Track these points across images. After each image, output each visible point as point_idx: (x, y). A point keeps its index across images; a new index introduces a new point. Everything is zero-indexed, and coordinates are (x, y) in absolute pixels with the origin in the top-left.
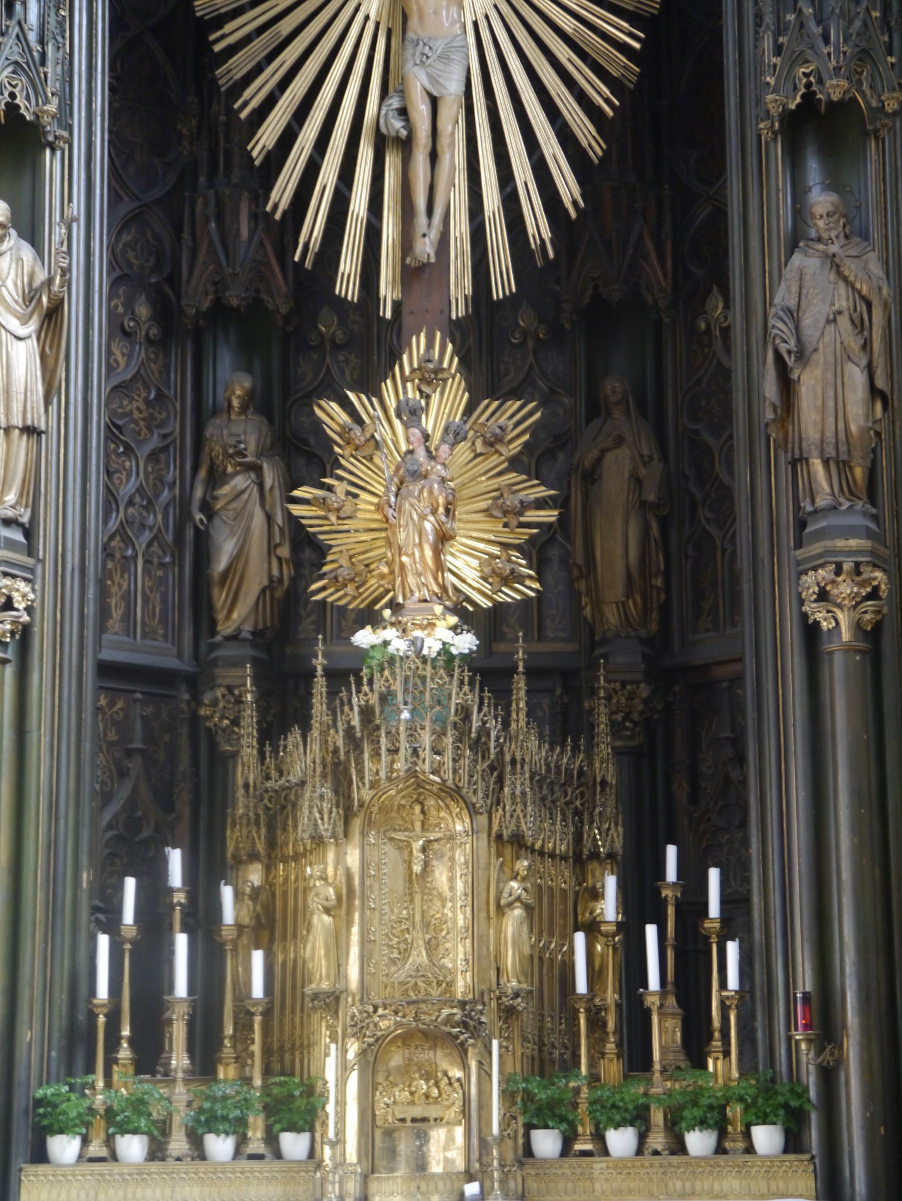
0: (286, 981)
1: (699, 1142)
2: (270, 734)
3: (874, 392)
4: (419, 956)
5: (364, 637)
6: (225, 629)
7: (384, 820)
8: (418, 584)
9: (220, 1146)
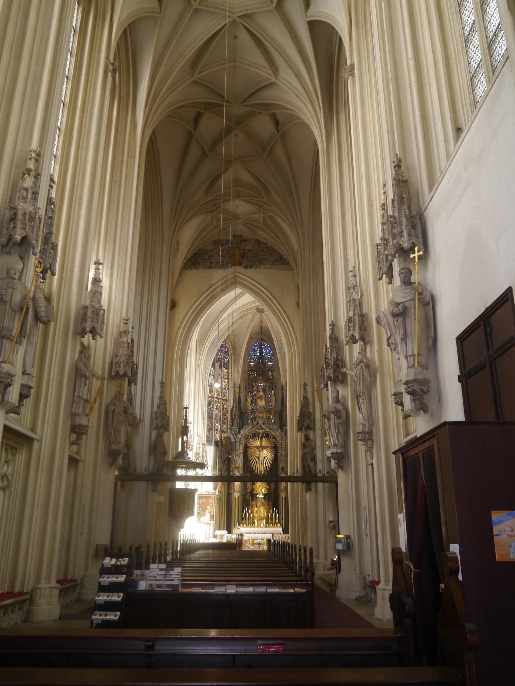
0: (253, 516)
7: (258, 507)
8: (260, 492)
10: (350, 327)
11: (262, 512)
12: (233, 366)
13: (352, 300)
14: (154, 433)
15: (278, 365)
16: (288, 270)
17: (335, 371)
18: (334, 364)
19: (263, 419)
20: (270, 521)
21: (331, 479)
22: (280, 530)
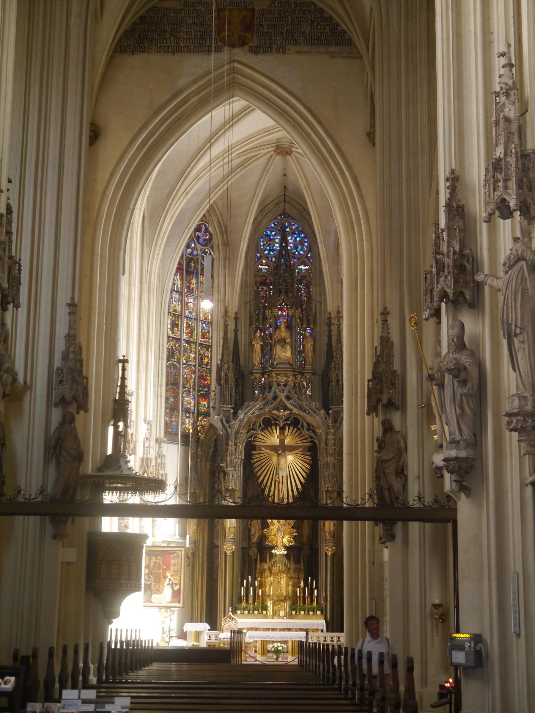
0: (264, 593)
1: (311, 613)
2: (261, 562)
3: (334, 525)
4: (279, 591)
5: (273, 551)
6: (253, 542)
7: (275, 575)
8: (279, 543)
9: (256, 612)
10: (496, 181)
11: (284, 586)
12: (222, 274)
13: (502, 123)
14: (56, 415)
15: (321, 272)
16: (349, 57)
17: (456, 282)
18: (455, 266)
19: (288, 388)
20: (299, 603)
21: (441, 515)
22: (321, 623)
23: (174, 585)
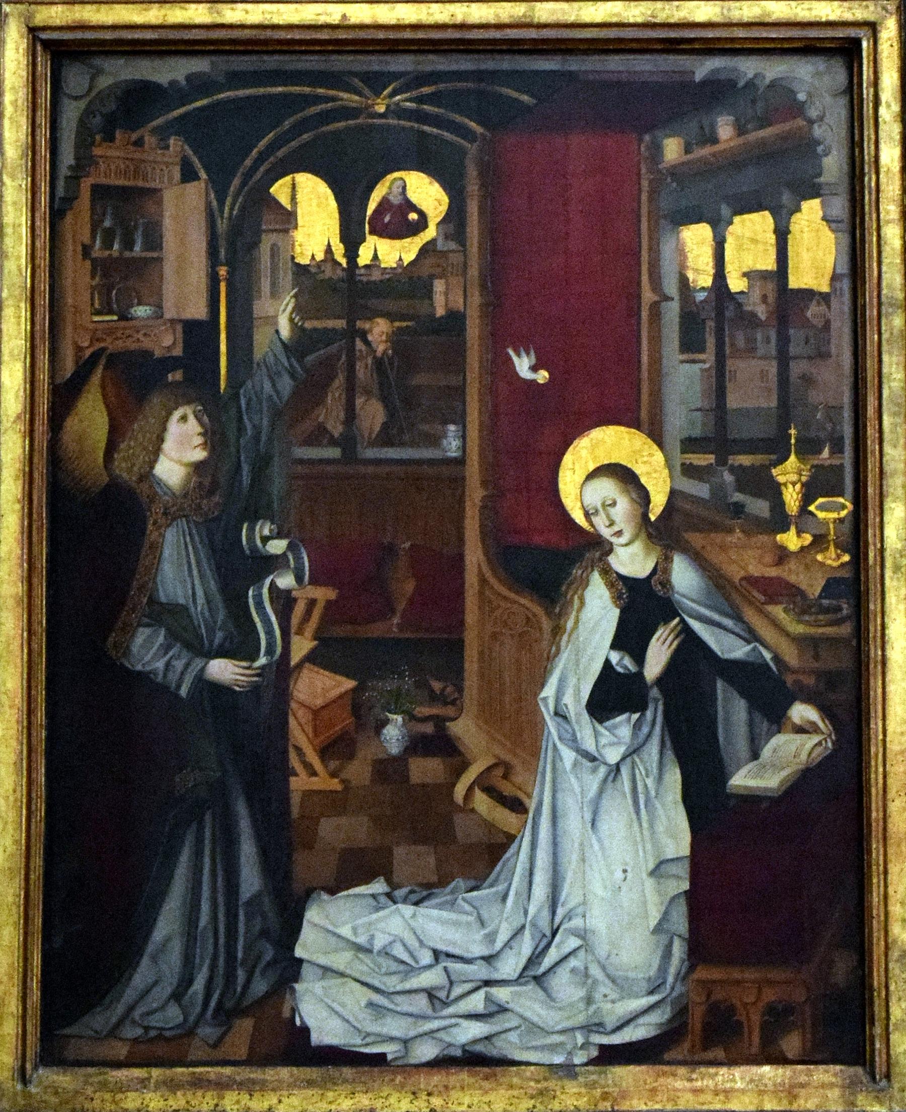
23: (733, 711)
